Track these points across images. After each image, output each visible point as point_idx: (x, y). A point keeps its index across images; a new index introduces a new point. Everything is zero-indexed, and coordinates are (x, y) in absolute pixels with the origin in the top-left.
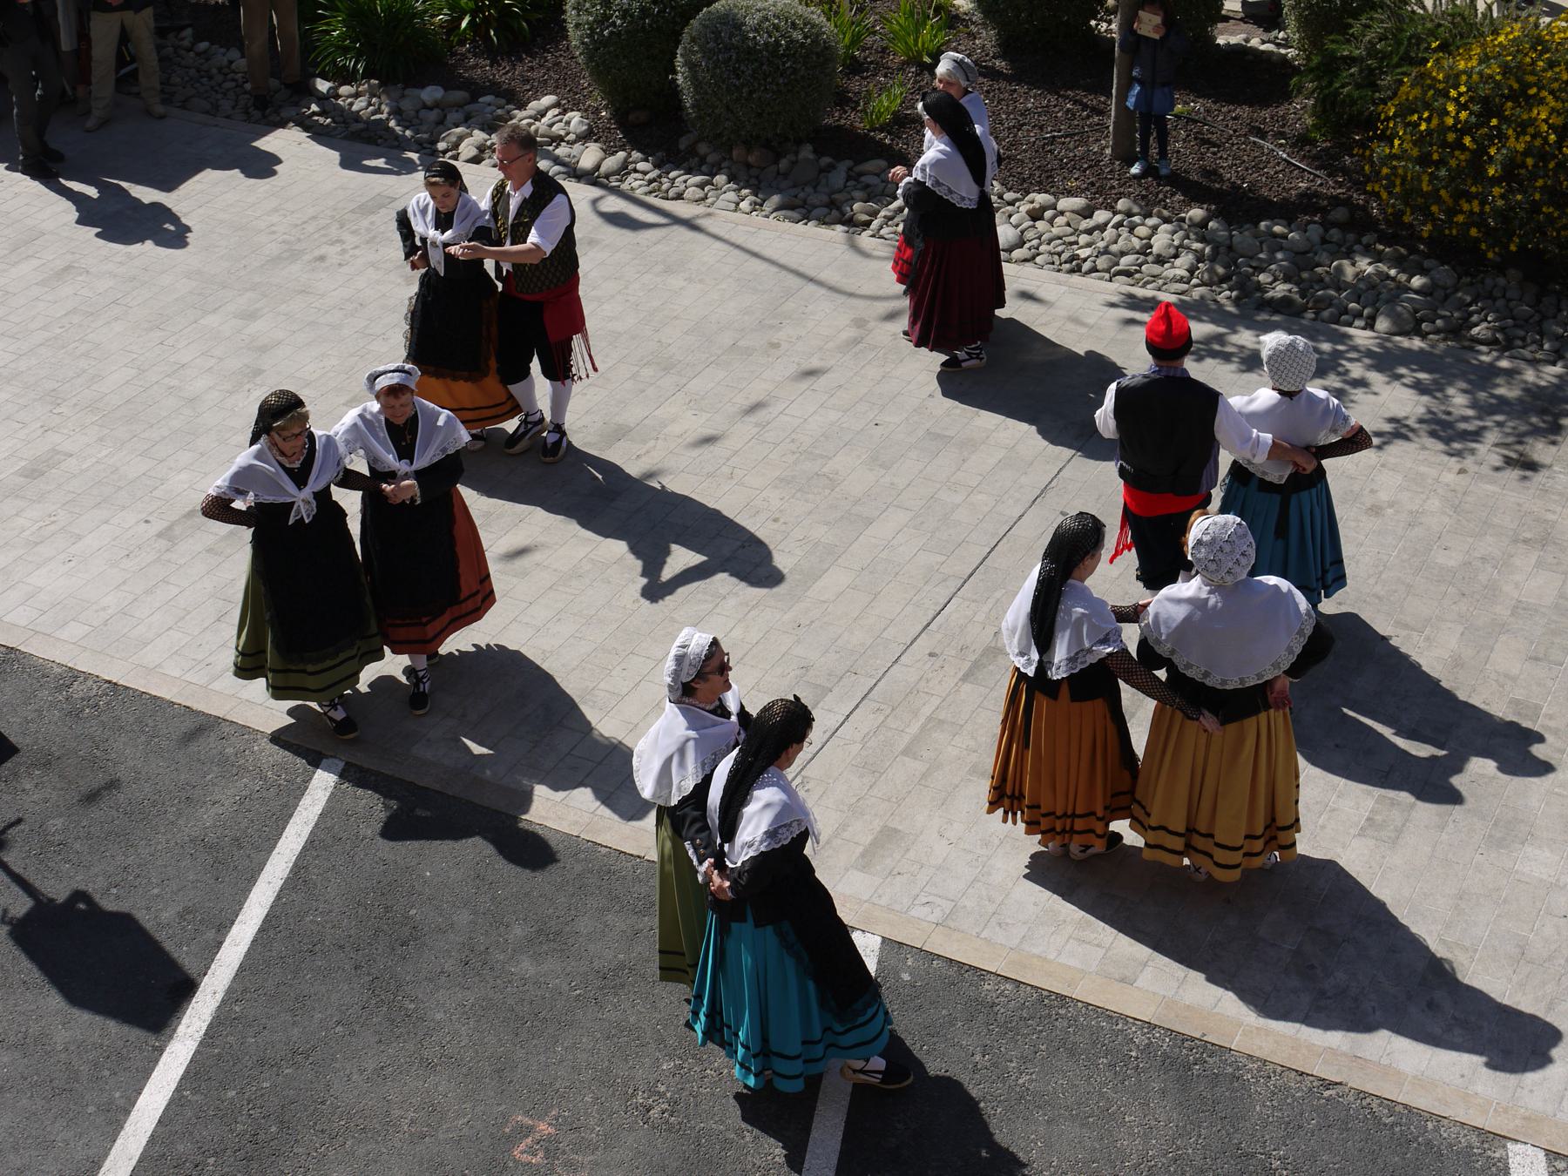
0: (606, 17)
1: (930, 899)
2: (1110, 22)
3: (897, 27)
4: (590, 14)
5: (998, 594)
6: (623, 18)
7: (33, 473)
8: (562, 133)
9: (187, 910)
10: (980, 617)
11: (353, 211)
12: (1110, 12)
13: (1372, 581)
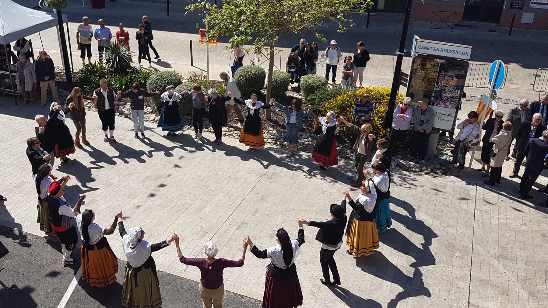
0: (156, 87)
1: (230, 279)
2: (264, 91)
3: (220, 91)
4: (153, 86)
5: (244, 211)
6: (160, 87)
7: (17, 187)
8: (146, 112)
9: (54, 289)
10: (240, 216)
11: (97, 128)
12: (264, 88)
13: (323, 207)
